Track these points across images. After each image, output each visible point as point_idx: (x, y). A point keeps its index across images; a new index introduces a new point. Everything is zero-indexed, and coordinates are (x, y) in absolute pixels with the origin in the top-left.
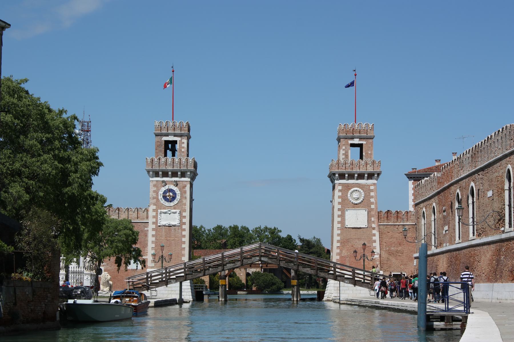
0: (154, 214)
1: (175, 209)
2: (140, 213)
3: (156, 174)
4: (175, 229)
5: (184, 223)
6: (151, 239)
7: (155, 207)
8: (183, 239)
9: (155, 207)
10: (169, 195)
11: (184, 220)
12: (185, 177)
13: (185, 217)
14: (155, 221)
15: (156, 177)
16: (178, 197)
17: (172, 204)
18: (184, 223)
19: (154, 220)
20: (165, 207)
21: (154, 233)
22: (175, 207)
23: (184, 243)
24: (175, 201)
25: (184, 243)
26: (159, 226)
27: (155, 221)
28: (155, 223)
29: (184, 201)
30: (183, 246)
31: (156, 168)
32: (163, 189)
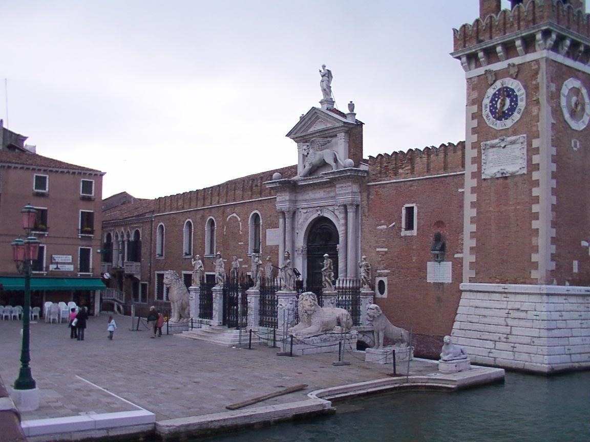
0: (474, 153)
1: (515, 133)
2: (450, 154)
3: (472, 58)
4: (516, 185)
5: (537, 167)
6: (469, 213)
7: (475, 138)
8: (535, 208)
9: (475, 138)
10: (503, 105)
11: (536, 159)
12: (535, 51)
13: (537, 151)
14: (475, 170)
15: (477, 67)
16: (522, 104)
17: (509, 123)
18: (537, 167)
19: (474, 168)
20: (495, 134)
21: (474, 198)
22: (515, 131)
23: (536, 216)
24: (515, 114)
25: (536, 216)
26: (484, 179)
27: (475, 170)
28: (477, 175)
29: (535, 110)
30: (535, 224)
31: (473, 47)
32: (491, 92)
